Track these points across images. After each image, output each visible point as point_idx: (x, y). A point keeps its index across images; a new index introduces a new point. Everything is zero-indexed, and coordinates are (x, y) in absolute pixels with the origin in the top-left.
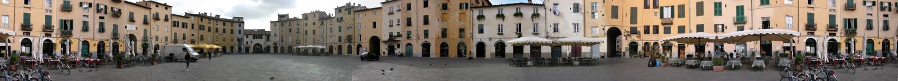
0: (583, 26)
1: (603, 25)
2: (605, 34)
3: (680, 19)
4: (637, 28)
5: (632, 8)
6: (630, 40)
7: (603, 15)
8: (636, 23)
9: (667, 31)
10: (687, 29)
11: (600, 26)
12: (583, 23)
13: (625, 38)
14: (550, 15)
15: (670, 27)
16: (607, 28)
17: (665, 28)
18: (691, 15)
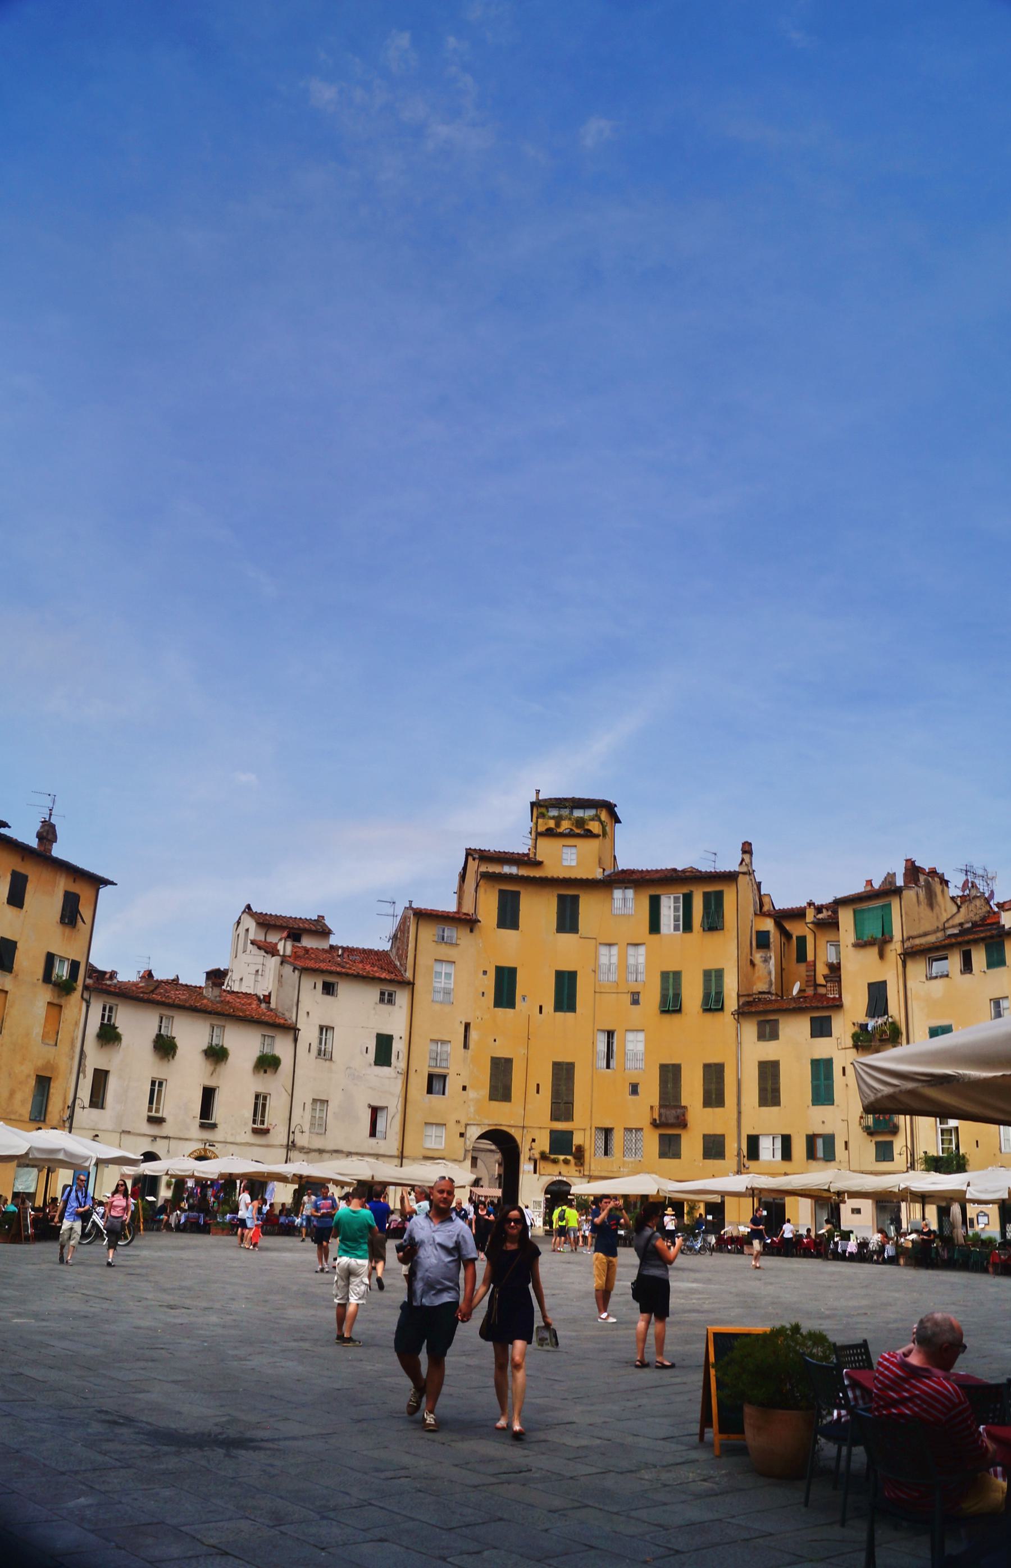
0: (399, 1118)
1: (463, 1122)
2: (466, 1151)
3: (709, 1110)
4: (570, 1134)
5: (557, 1066)
6: (551, 1174)
7: (464, 1088)
8: (569, 1116)
9: (670, 1148)
10: (731, 1147)
11: (451, 1124)
12: (400, 1108)
13: (532, 1167)
14: (307, 1060)
15: (679, 1136)
16: (474, 1132)
17: (661, 1136)
18: (743, 1101)
